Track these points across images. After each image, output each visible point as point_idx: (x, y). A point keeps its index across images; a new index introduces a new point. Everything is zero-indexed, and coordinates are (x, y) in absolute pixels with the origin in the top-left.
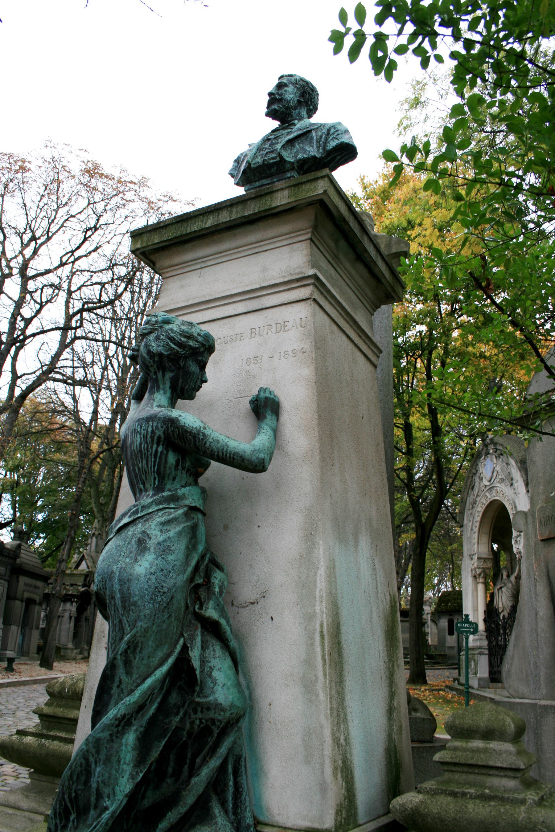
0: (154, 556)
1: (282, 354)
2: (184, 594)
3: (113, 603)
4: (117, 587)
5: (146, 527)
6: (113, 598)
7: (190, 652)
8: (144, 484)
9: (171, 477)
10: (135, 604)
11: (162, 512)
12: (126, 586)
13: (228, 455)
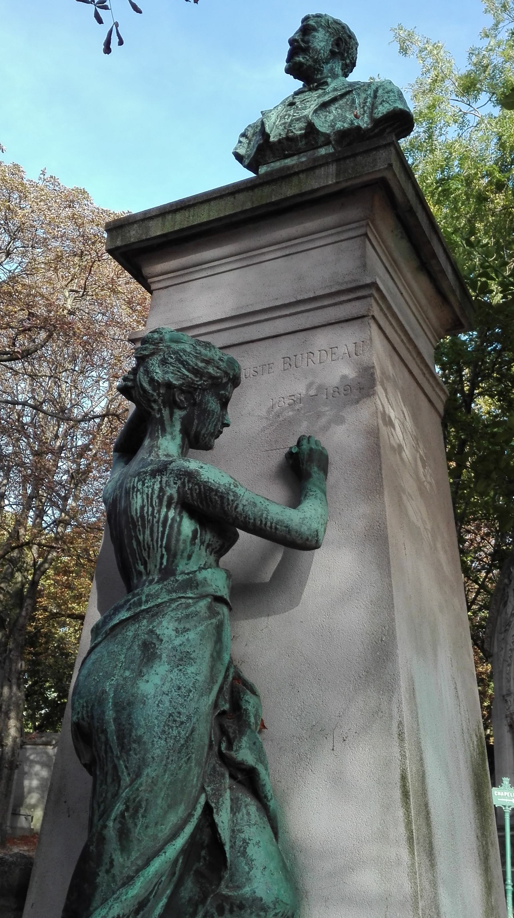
0: (167, 667)
2: (209, 725)
3: (103, 738)
4: (110, 714)
5: (155, 624)
6: (104, 731)
7: (215, 816)
8: (145, 564)
9: (185, 555)
10: (139, 740)
11: (177, 604)
12: (126, 713)
13: (269, 524)
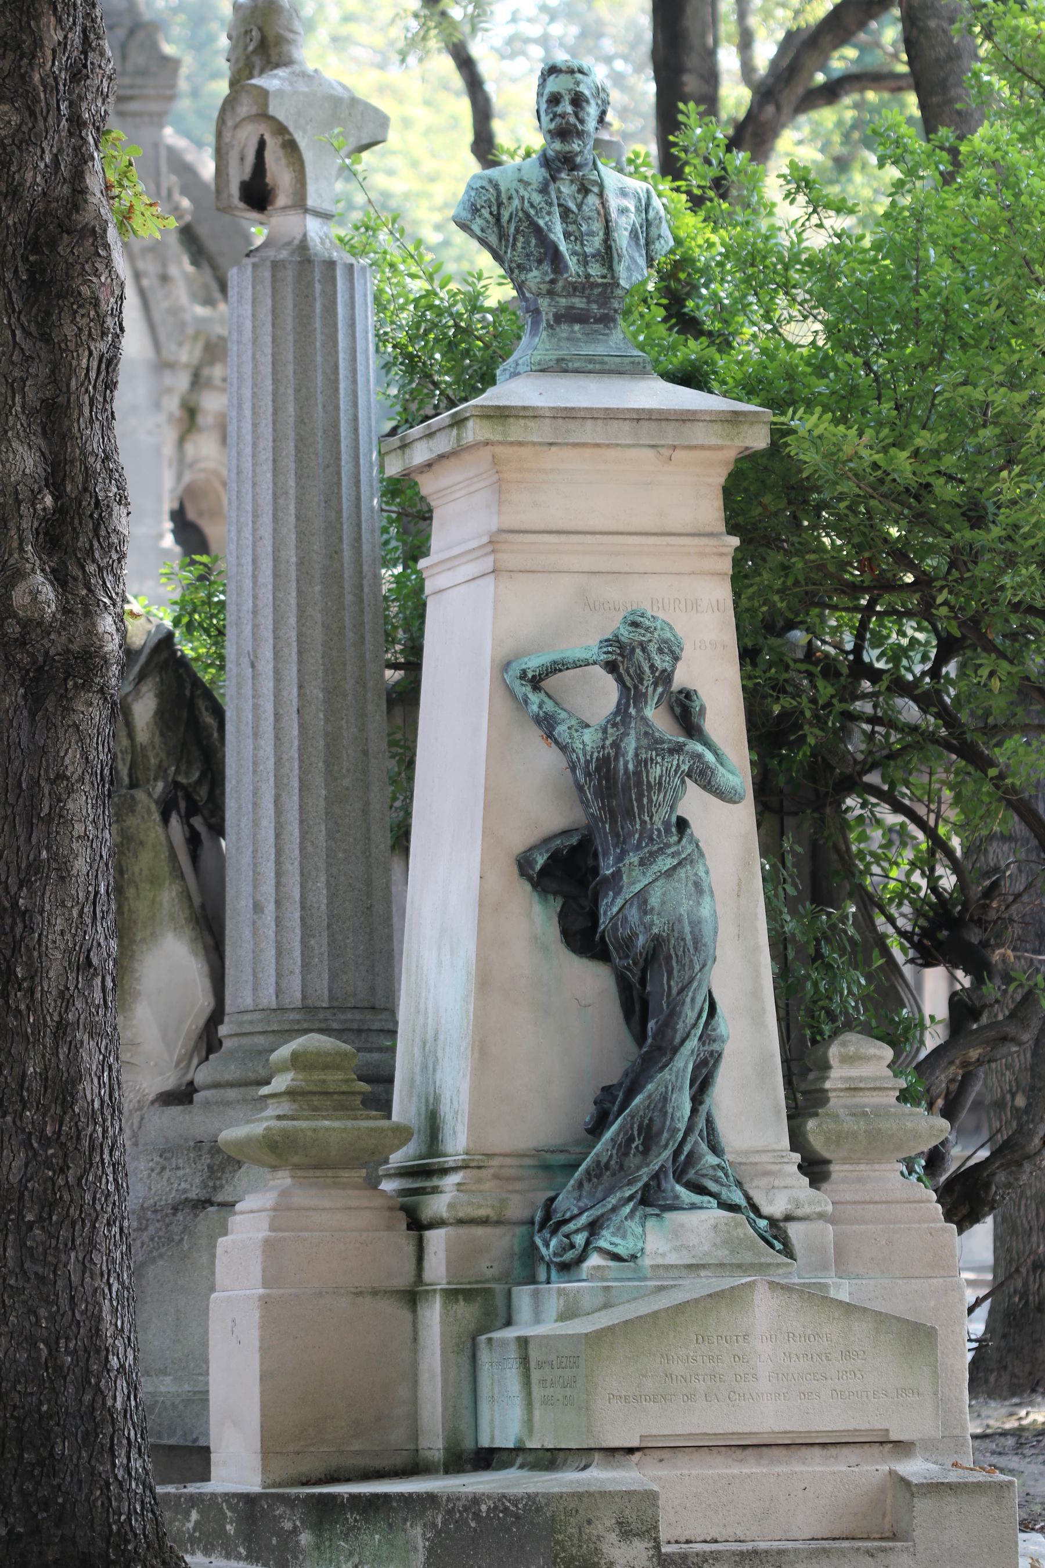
1: (698, 644)
4: (687, 929)
